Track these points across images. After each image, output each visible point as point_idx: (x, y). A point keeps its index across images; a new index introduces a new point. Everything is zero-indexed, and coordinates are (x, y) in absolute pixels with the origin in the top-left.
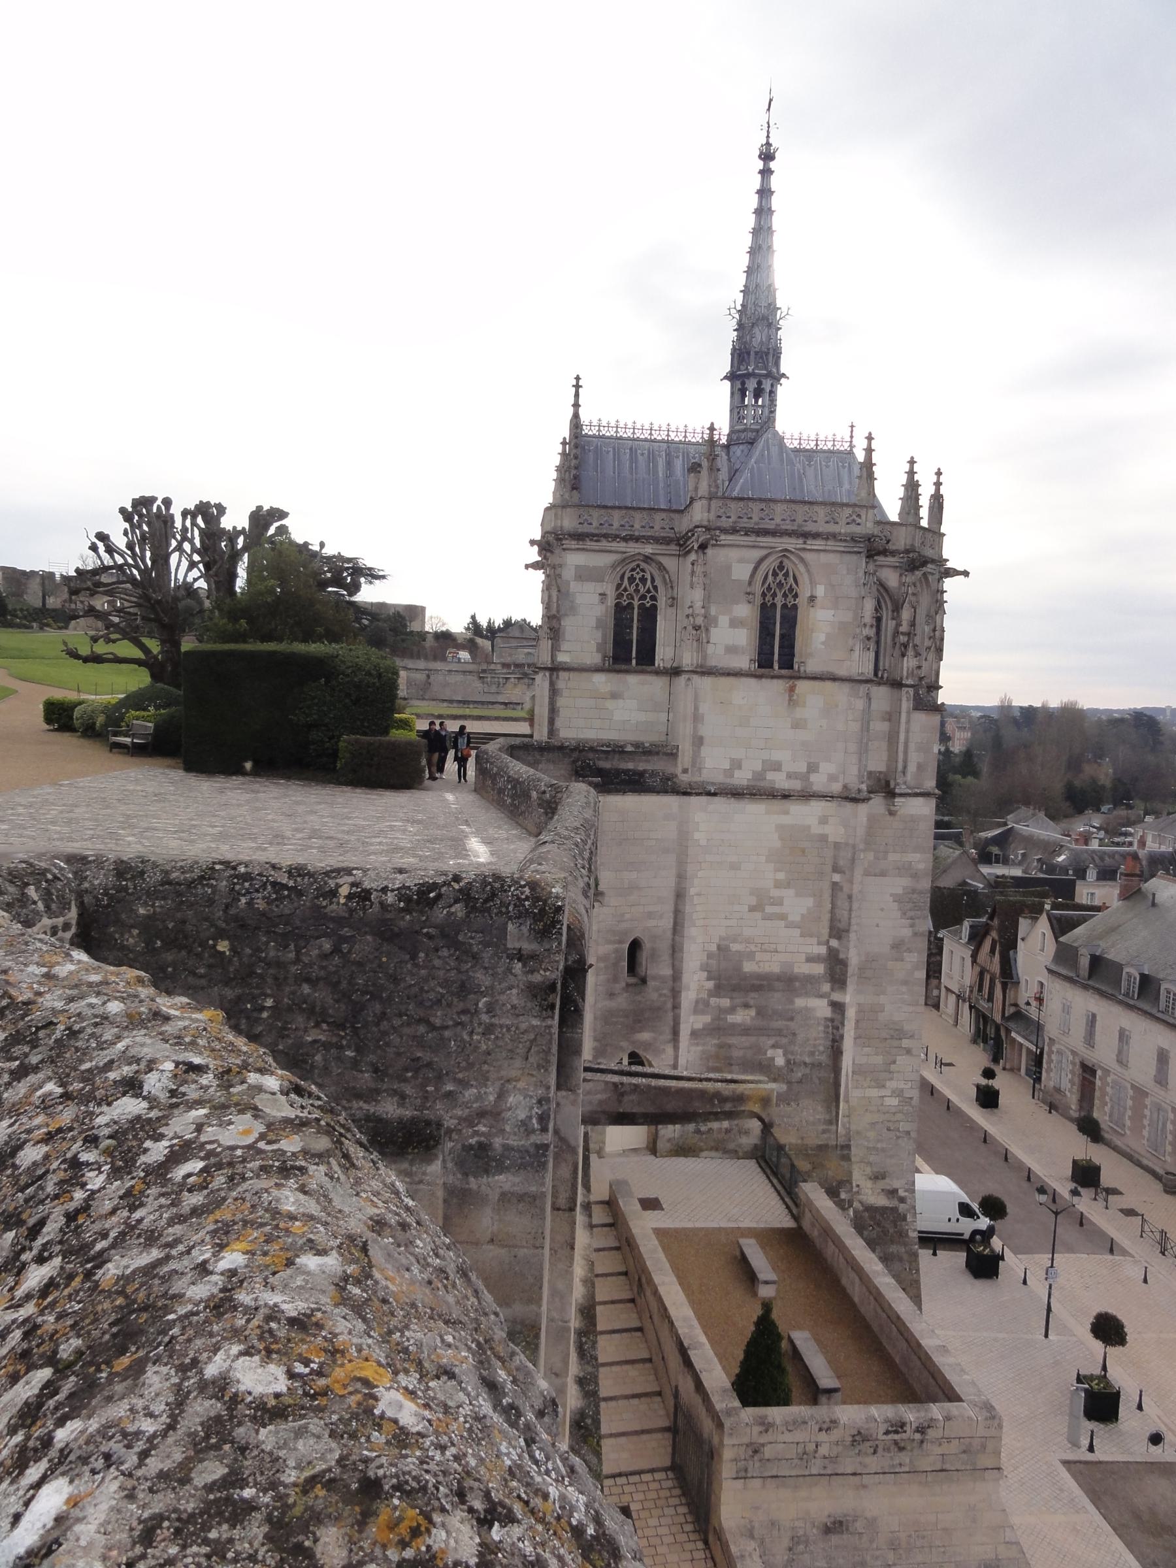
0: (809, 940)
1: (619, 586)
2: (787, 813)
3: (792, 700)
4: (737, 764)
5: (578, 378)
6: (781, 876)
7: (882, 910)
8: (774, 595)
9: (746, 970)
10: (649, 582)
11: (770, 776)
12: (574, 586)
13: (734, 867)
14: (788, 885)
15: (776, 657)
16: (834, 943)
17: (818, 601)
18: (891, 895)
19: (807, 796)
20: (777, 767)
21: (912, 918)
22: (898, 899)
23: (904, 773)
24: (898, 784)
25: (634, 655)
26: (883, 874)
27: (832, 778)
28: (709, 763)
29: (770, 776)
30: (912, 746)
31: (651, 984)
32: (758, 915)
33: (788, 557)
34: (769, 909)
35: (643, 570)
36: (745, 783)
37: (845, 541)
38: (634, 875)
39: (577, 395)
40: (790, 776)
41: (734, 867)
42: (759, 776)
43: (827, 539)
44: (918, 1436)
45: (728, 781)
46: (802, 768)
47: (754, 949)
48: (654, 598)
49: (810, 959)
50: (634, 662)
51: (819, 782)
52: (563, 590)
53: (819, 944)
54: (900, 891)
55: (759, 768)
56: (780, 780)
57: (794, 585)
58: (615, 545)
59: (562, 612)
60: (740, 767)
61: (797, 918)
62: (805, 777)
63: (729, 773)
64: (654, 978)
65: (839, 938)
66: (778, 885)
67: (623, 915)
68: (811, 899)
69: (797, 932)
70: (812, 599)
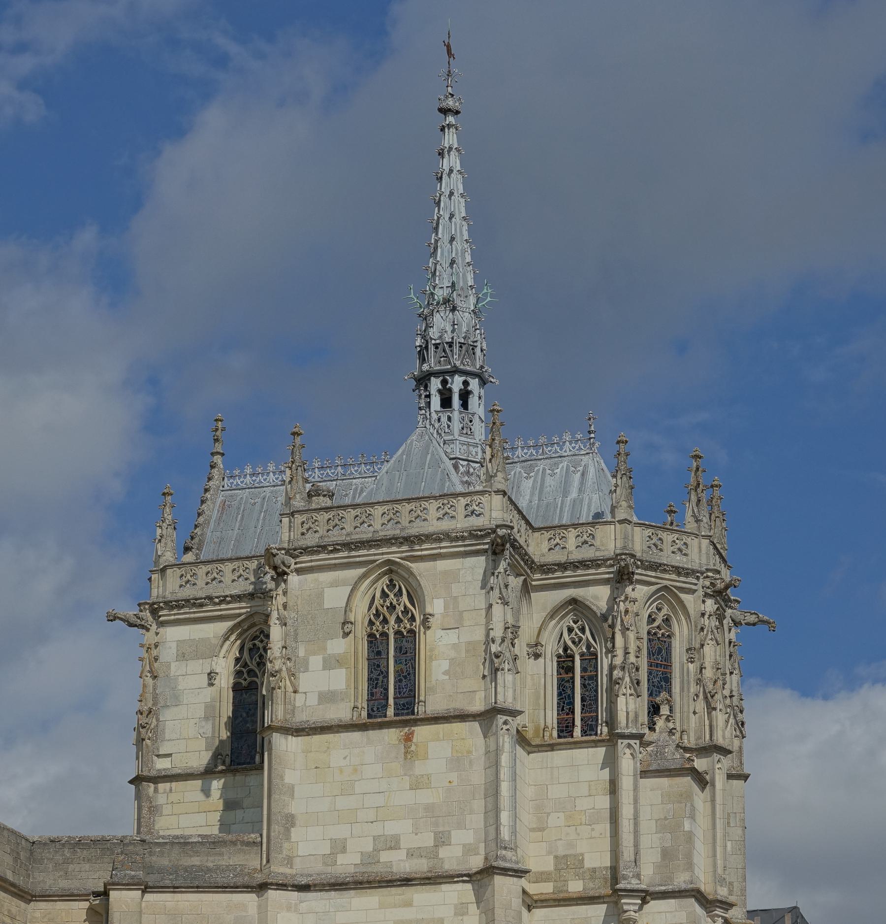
1: (237, 660)
2: (409, 904)
3: (409, 751)
8: (385, 621)
11: (385, 857)
12: (176, 669)
15: (391, 701)
20: (393, 844)
24: (625, 878)
27: (469, 850)
28: (303, 849)
29: (385, 857)
30: (647, 826)
36: (352, 870)
37: (463, 538)
40: (410, 854)
42: (370, 858)
43: (440, 540)
45: (329, 869)
46: (427, 840)
51: (451, 858)
56: (398, 862)
59: (162, 703)
60: (344, 850)
62: (432, 853)
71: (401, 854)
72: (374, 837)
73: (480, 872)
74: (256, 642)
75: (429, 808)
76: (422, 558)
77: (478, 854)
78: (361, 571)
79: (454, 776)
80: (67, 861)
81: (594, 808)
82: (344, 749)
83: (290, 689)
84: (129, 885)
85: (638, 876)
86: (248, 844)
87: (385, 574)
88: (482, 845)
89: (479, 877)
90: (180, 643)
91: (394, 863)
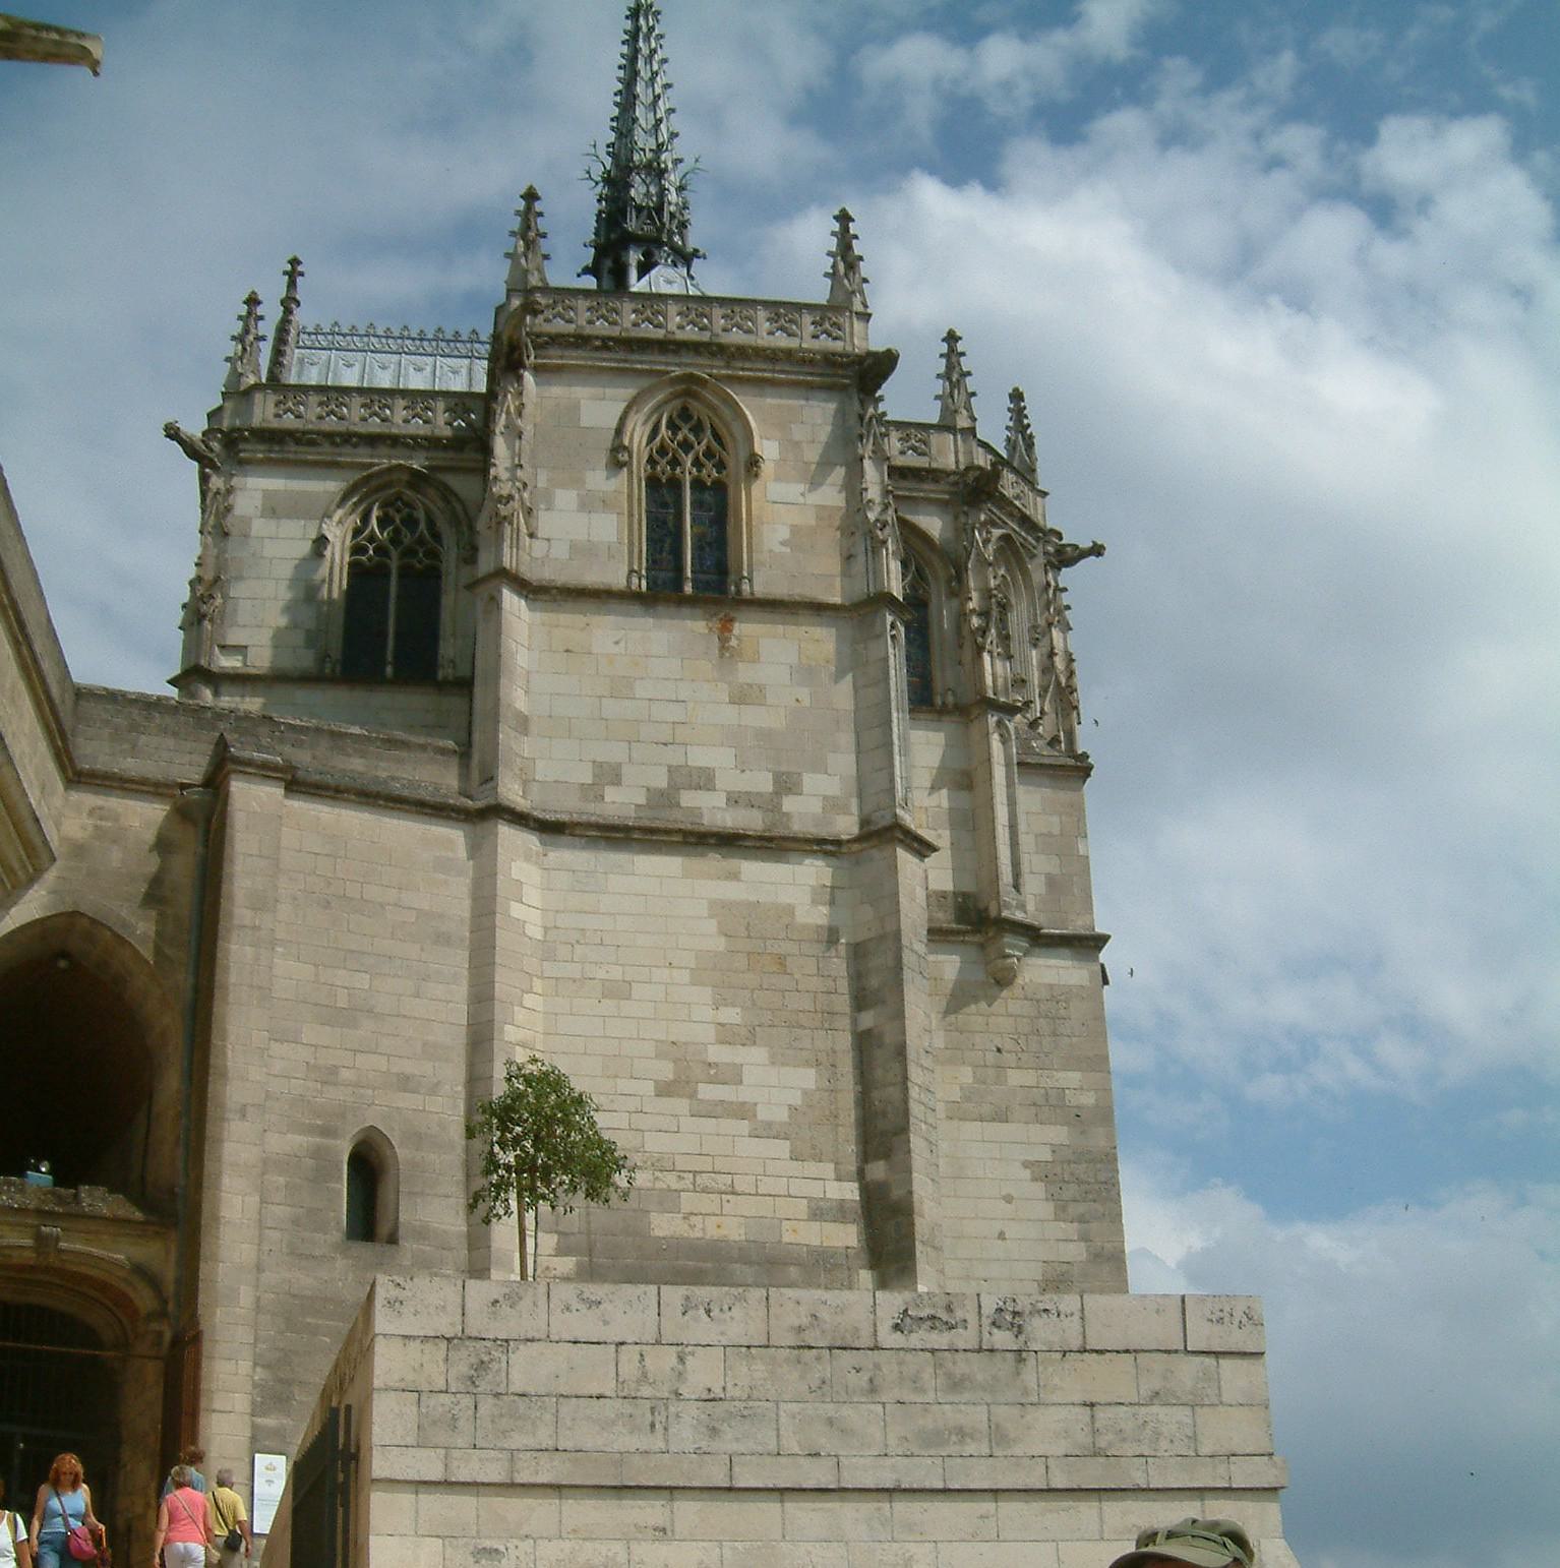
0: (812, 1168)
1: (357, 532)
2: (735, 876)
4: (609, 774)
5: (295, 262)
6: (732, 1015)
7: (1008, 1199)
8: (675, 462)
9: (658, 1233)
10: (422, 526)
11: (688, 799)
12: (259, 527)
13: (617, 991)
14: (751, 1039)
16: (878, 1170)
17: (767, 469)
18: (1026, 1165)
19: (774, 845)
20: (704, 780)
21: (1081, 1219)
22: (1043, 1173)
23: (1017, 886)
24: (1007, 906)
25: (389, 657)
26: (1001, 1116)
27: (832, 805)
28: (543, 771)
29: (688, 799)
30: (1026, 841)
31: (408, 1246)
32: (681, 1105)
33: (695, 396)
34: (707, 1092)
35: (407, 505)
38: (362, 981)
39: (292, 285)
40: (734, 800)
41: (617, 991)
42: (664, 798)
44: (1003, 1339)
46: (764, 783)
47: (674, 1186)
48: (433, 555)
49: (819, 1212)
50: (389, 670)
51: (803, 811)
52: (234, 531)
53: (839, 1179)
54: (1046, 1155)
55: (661, 781)
56: (712, 810)
57: (715, 445)
58: (347, 455)
60: (617, 781)
61: (783, 1115)
63: (593, 791)
64: (422, 1234)
65: (887, 1155)
66: (727, 1035)
67: (334, 1070)
68: (812, 1072)
69: (783, 1148)
70: (753, 463)
71: (718, 799)
72: (670, 767)
73: (857, 840)
74: (391, 511)
75: (765, 735)
76: (740, 380)
77: (852, 814)
78: (645, 382)
79: (804, 694)
80: (133, 727)
81: (939, 806)
82: (613, 636)
83: (523, 530)
84: (266, 771)
85: (1022, 907)
86: (443, 751)
87: (676, 396)
88: (854, 803)
89: (856, 847)
90: (267, 495)
91: (705, 811)
